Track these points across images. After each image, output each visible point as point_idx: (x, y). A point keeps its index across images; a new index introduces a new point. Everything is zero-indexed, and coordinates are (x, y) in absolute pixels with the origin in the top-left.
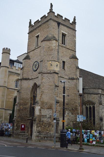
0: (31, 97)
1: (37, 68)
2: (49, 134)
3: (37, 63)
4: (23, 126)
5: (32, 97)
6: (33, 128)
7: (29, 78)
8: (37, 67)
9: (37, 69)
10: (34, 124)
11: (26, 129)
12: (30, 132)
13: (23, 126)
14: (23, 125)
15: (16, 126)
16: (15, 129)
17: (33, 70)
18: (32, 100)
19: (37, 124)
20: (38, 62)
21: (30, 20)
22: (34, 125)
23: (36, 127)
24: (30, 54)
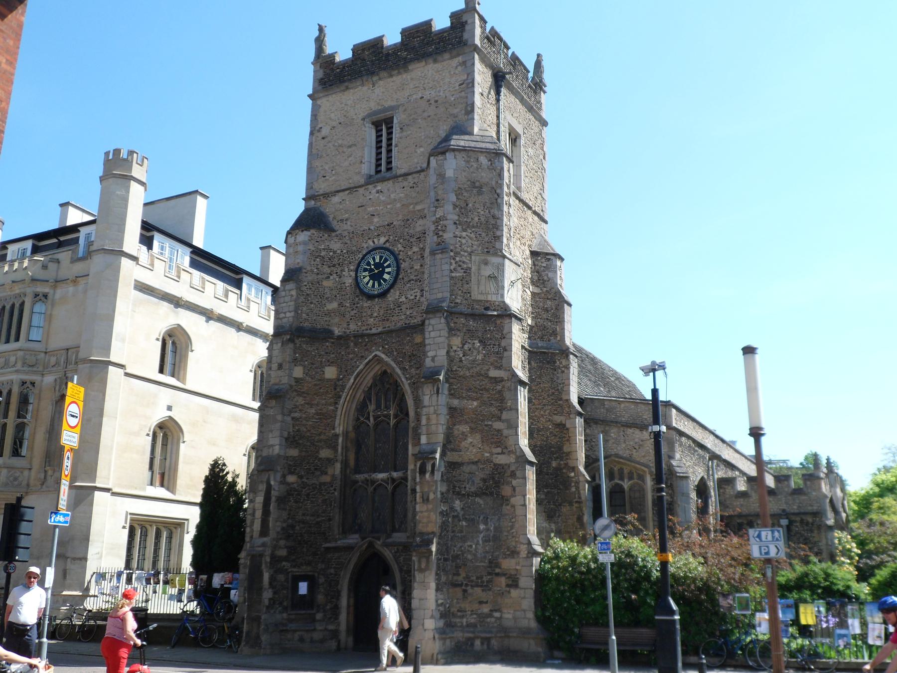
0: (347, 432)
1: (385, 286)
2: (493, 620)
3: (386, 255)
4: (303, 588)
5: (351, 428)
6: (416, 593)
7: (331, 332)
8: (386, 276)
9: (392, 286)
10: (421, 570)
11: (320, 598)
12: (348, 613)
13: (303, 588)
14: (303, 578)
15: (270, 583)
16: (266, 602)
17: (362, 293)
18: (349, 444)
19: (437, 574)
20: (392, 253)
21: (321, 29)
22: (418, 576)
23: (433, 585)
24: (331, 208)
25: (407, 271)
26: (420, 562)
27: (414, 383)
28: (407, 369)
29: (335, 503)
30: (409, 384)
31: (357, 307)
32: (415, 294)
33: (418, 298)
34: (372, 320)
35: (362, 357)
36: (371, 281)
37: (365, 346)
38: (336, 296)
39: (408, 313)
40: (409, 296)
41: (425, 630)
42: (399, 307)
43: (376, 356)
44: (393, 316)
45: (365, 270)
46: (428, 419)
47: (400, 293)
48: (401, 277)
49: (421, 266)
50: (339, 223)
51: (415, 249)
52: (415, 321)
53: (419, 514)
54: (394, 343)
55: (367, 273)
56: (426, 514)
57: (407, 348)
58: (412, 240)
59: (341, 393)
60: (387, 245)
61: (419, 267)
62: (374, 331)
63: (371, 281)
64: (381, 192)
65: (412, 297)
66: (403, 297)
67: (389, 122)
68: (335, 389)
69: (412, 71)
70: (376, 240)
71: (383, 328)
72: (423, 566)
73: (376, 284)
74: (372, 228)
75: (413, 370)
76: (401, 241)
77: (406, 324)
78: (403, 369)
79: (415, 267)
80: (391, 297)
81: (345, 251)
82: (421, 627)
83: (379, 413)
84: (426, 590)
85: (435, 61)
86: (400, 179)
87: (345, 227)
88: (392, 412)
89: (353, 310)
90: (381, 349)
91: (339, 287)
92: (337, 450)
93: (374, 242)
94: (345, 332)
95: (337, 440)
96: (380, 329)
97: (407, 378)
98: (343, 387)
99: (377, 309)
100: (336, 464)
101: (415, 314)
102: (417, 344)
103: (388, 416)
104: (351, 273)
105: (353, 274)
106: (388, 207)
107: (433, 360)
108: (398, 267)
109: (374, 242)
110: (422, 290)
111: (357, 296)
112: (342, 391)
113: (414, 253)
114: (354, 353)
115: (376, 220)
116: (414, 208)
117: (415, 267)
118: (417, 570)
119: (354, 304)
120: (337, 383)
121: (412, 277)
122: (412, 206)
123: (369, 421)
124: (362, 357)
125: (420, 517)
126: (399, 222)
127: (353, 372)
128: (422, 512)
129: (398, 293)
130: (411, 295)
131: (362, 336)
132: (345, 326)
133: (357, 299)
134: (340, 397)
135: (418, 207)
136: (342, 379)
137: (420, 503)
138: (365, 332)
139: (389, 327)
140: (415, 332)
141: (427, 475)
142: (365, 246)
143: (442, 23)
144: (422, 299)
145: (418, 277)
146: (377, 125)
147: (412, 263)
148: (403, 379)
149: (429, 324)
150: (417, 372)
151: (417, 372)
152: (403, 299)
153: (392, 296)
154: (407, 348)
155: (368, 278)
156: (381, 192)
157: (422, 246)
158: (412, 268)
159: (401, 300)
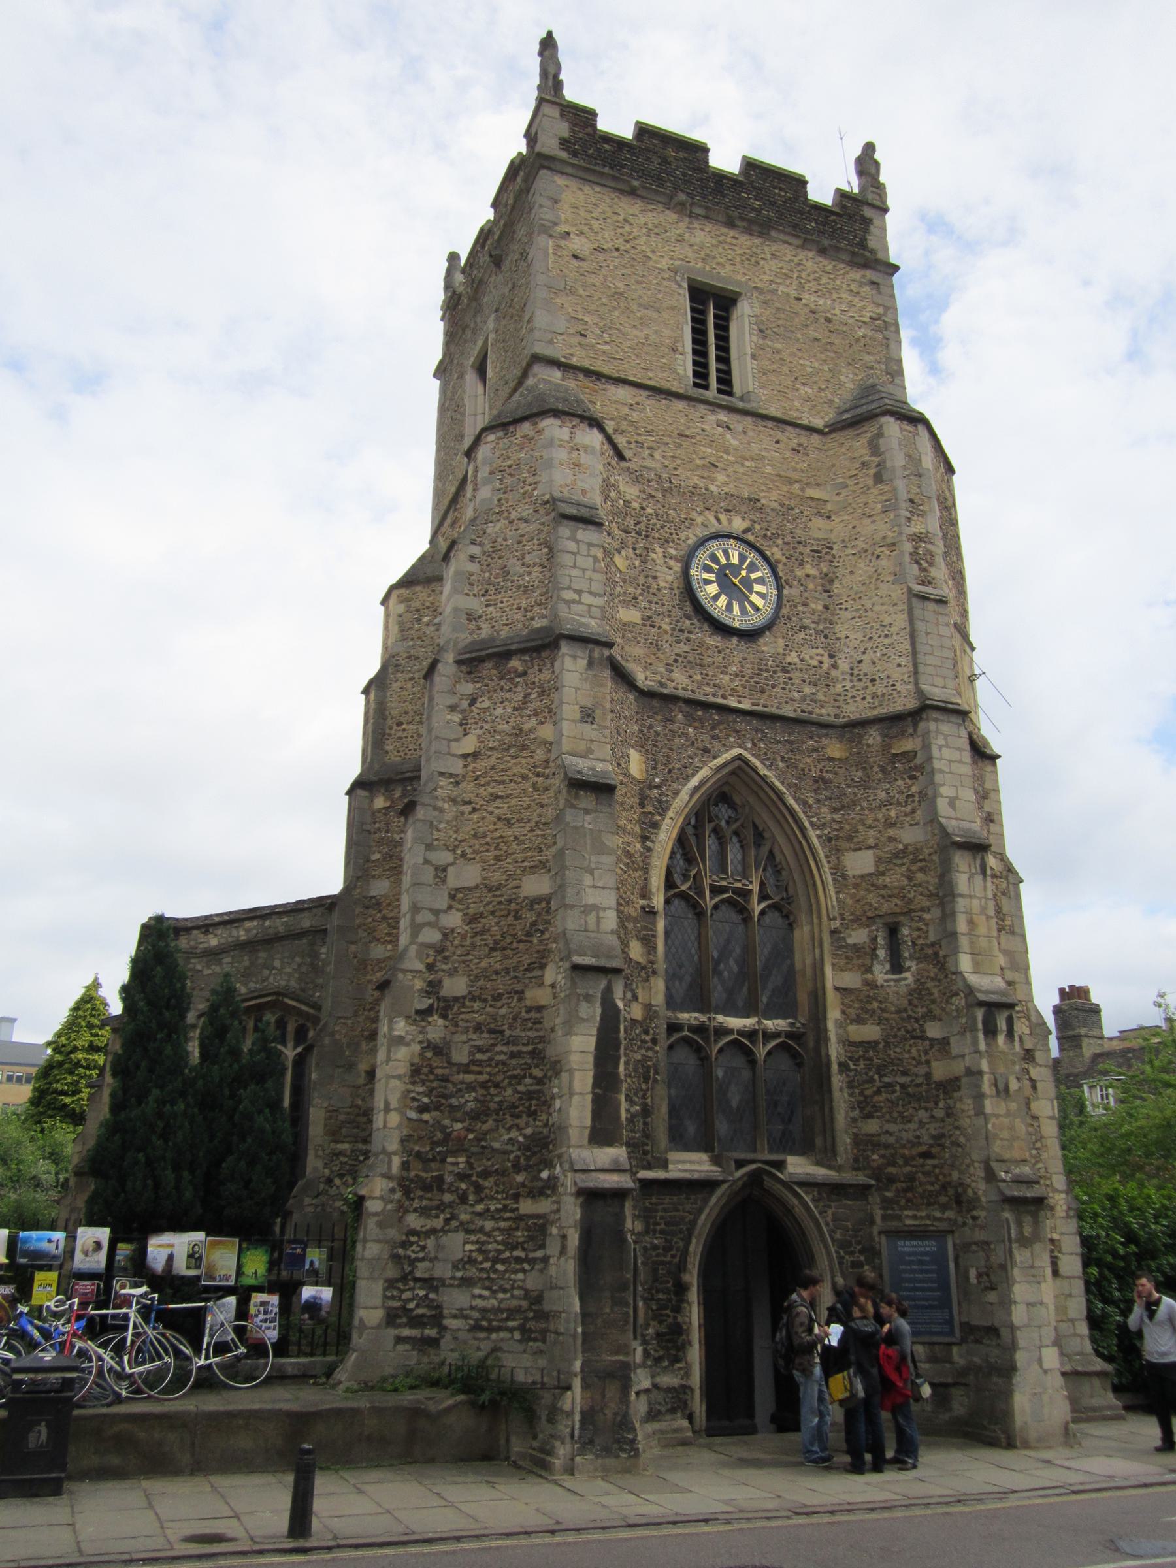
1: (755, 620)
3: (752, 556)
25: (795, 607)
26: (1019, 1224)
27: (830, 840)
28: (810, 807)
29: (656, 1073)
30: (819, 837)
31: (688, 640)
32: (819, 658)
33: (825, 666)
34: (727, 678)
35: (706, 751)
36: (723, 597)
37: (713, 728)
38: (635, 598)
39: (808, 690)
40: (807, 658)
41: (1046, 1372)
42: (788, 672)
43: (740, 757)
44: (773, 686)
45: (708, 569)
46: (971, 922)
47: (787, 646)
48: (784, 611)
49: (826, 607)
50: (633, 446)
51: (809, 569)
52: (823, 711)
53: (993, 1120)
54: (779, 742)
55: (712, 577)
56: (1006, 1120)
57: (808, 761)
58: (801, 549)
59: (658, 818)
60: (750, 537)
61: (820, 608)
62: (732, 702)
63: (723, 597)
64: (728, 428)
65: (815, 663)
66: (794, 654)
67: (726, 302)
68: (643, 806)
69: (775, 241)
70: (722, 517)
71: (753, 704)
72: (1028, 1231)
73: (736, 609)
74: (712, 488)
75: (824, 810)
76: (779, 541)
77: (803, 711)
78: (805, 804)
79: (813, 605)
80: (765, 644)
81: (649, 511)
82: (1036, 1367)
83: (724, 883)
84: (1039, 1283)
85: (822, 251)
86: (770, 424)
87: (649, 463)
88: (755, 887)
89: (678, 642)
90: (749, 745)
91: (642, 580)
92: (655, 948)
93: (718, 519)
94: (662, 685)
95: (654, 923)
96: (746, 705)
97: (812, 824)
98: (663, 809)
99: (736, 660)
100: (652, 980)
101: (820, 696)
102: (831, 759)
103: (746, 894)
104: (672, 563)
105: (677, 567)
106: (747, 463)
107: (952, 803)
108: (780, 588)
109: (718, 519)
110: (831, 656)
111: (688, 617)
112: (661, 815)
113: (808, 576)
114: (685, 735)
115: (721, 477)
116: (802, 489)
117: (813, 605)
118: (1018, 1241)
119: (681, 631)
120: (648, 792)
121: (806, 622)
122: (797, 486)
123: (701, 893)
124: (706, 751)
125: (994, 1125)
126: (775, 505)
127: (687, 779)
128: (997, 1116)
129: (781, 642)
130: (812, 658)
131: (706, 706)
132: (662, 670)
133: (688, 622)
134: (655, 825)
135: (811, 492)
136: (657, 787)
137: (992, 1096)
138: (711, 699)
139: (764, 706)
140: (827, 735)
141: (1001, 1039)
142: (700, 520)
143: (821, 193)
144: (833, 673)
145: (821, 627)
146: (699, 294)
147: (806, 595)
148: (807, 824)
149: (937, 731)
150: (835, 817)
151: (835, 817)
152: (793, 657)
153: (769, 645)
154: (808, 761)
155: (713, 589)
156: (728, 428)
157: (825, 570)
158: (805, 604)
159: (789, 659)
